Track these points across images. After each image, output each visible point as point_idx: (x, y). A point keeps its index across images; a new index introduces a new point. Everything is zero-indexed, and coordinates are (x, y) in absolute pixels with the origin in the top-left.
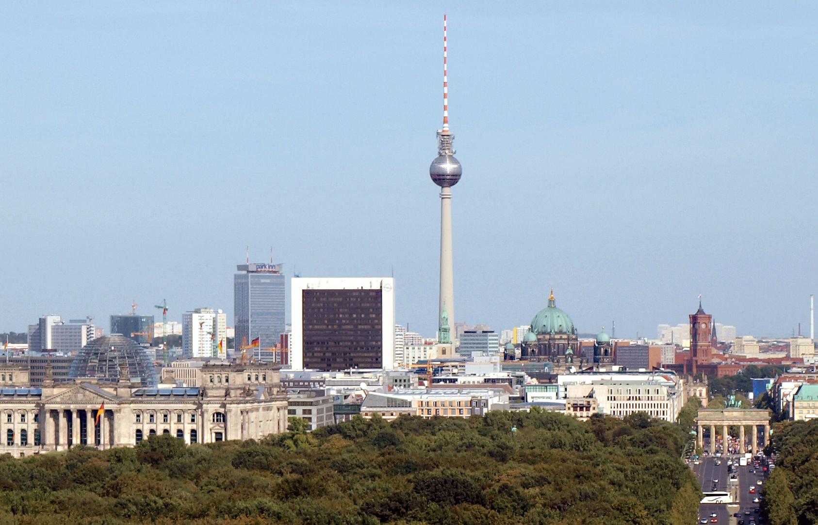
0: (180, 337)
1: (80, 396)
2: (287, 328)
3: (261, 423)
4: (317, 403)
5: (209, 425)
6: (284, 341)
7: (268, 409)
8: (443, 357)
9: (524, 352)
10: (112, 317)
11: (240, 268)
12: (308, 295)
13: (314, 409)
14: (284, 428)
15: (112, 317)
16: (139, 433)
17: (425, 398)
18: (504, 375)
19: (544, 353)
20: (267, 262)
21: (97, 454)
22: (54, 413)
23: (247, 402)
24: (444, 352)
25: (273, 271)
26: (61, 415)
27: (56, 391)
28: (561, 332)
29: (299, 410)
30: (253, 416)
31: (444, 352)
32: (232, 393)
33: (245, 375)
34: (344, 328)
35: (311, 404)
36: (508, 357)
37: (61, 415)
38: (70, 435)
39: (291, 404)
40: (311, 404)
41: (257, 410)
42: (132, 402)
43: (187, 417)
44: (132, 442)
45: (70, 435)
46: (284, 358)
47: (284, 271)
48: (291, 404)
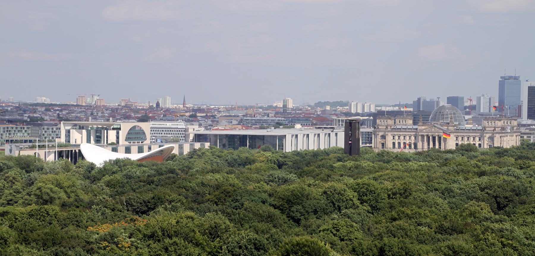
0: (475, 106)
1: (433, 130)
3: (510, 142)
5: (486, 142)
6: (520, 108)
7: (512, 136)
10: (449, 98)
11: (501, 77)
12: (530, 88)
13: (532, 137)
14: (519, 144)
15: (449, 98)
16: (457, 144)
20: (513, 75)
21: (440, 152)
22: (423, 136)
23: (502, 133)
25: (516, 78)
26: (425, 137)
27: (423, 127)
29: (525, 137)
30: (505, 139)
32: (497, 129)
33: (502, 122)
35: (531, 134)
37: (425, 137)
38: (429, 144)
40: (531, 134)
41: (507, 136)
43: (477, 139)
44: (454, 147)
45: (429, 144)
46: (520, 115)
47: (520, 79)
48: (522, 134)
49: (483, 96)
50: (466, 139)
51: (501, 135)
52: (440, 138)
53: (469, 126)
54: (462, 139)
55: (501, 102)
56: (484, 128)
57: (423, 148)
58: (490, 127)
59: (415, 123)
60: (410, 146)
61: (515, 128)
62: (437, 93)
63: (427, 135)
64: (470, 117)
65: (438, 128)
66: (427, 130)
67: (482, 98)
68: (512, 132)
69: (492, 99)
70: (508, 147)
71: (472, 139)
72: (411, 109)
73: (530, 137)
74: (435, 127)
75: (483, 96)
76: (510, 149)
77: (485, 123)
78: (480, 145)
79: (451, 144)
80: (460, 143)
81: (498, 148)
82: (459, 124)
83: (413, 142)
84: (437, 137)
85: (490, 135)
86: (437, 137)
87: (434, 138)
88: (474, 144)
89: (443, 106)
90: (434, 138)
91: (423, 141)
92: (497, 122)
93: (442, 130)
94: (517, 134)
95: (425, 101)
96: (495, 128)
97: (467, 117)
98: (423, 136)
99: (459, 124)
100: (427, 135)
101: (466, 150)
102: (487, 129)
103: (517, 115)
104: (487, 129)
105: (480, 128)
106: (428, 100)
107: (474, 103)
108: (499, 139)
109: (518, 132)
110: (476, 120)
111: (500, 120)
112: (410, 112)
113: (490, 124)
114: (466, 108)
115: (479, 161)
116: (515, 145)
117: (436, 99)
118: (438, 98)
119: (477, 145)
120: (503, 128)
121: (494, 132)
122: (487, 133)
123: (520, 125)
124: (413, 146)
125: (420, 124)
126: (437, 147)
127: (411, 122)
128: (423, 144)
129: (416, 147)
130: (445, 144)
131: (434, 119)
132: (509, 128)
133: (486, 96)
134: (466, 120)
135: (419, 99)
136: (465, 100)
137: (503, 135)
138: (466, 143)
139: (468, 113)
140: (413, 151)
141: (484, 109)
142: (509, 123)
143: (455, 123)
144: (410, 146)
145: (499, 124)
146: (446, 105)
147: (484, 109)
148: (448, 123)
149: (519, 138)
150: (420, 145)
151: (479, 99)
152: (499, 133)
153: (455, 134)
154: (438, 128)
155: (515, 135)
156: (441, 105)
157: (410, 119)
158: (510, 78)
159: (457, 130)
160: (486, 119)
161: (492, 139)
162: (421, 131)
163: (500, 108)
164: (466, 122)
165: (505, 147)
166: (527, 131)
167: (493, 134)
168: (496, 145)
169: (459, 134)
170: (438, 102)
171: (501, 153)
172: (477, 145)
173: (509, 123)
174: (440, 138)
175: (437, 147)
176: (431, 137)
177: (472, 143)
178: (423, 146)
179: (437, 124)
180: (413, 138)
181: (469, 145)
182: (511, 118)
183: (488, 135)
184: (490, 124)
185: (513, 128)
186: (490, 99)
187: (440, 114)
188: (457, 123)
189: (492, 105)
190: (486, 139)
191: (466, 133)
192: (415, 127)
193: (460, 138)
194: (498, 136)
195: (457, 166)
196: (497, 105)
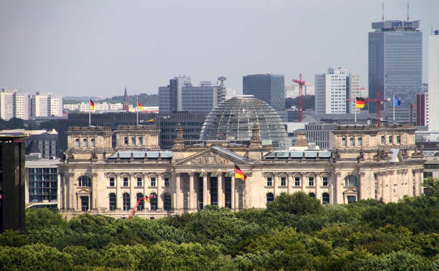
0: (313, 97)
1: (211, 160)
5: (341, 189)
7: (404, 172)
11: (375, 25)
14: (420, 191)
16: (270, 196)
20: (403, 19)
22: (185, 177)
23: (380, 165)
25: (410, 27)
27: (186, 155)
30: (387, 179)
32: (366, 156)
33: (379, 137)
38: (200, 198)
39: (426, 166)
41: (391, 173)
42: (264, 166)
43: (319, 181)
45: (200, 198)
47: (421, 28)
48: (426, 166)
49: (331, 72)
50: (291, 181)
51: (376, 170)
52: (227, 180)
53: (298, 150)
54: (283, 183)
55: (376, 87)
56: (336, 154)
57: (186, 208)
58: (350, 152)
59: (165, 144)
60: (154, 201)
61: (410, 153)
62: (219, 66)
63: (197, 175)
64: (301, 126)
65: (222, 155)
66: (196, 161)
67: (328, 78)
68: (404, 162)
69: (352, 80)
70: (395, 200)
71: (305, 181)
72: (155, 109)
74: (215, 152)
75: (331, 72)
76: (400, 206)
77: (338, 141)
78: (326, 196)
79: (256, 195)
80: (278, 192)
81: (371, 202)
82: (276, 145)
83: (160, 192)
84: (220, 179)
85: (351, 170)
86: (220, 179)
87: (213, 182)
88: (312, 195)
89: (234, 100)
90: (213, 182)
91: (185, 189)
92: (366, 137)
93: (232, 159)
94: (414, 167)
95: (188, 87)
97: (293, 127)
98: (185, 177)
99: (276, 145)
101: (290, 209)
102: (343, 156)
103: (415, 119)
104: (343, 156)
105: (325, 153)
106: (196, 84)
107: (310, 90)
108: (373, 181)
109: (418, 163)
110: (313, 134)
111: (373, 134)
112: (152, 115)
113: (349, 142)
114: (289, 102)
115: (325, 237)
116: (411, 195)
117: (214, 82)
118: (222, 79)
119: (319, 197)
120: (381, 154)
121: (359, 164)
122: (342, 166)
124: (161, 203)
125: (178, 146)
127: (152, 141)
128: (186, 196)
129: (168, 206)
130: (241, 196)
131: (212, 132)
132: (396, 152)
133: (337, 72)
134: (291, 135)
135: (174, 83)
136: (288, 83)
137: (382, 170)
138: (292, 191)
139: (295, 117)
140: (161, 215)
141: (333, 105)
142: (395, 140)
144: (154, 201)
145: (372, 142)
146: (241, 96)
147: (333, 105)
148: (248, 143)
149: (420, 177)
150: (178, 200)
151: (321, 81)
153: (265, 170)
154: (222, 155)
155: (410, 169)
156: (228, 97)
157: (153, 134)
158: (396, 25)
159: (271, 161)
160: (339, 131)
161: (354, 180)
163: (374, 101)
164: (290, 139)
165: (387, 201)
170: (221, 91)
171: (380, 215)
172: (319, 197)
173: (395, 140)
174: (227, 180)
175: (221, 203)
176: (205, 179)
178: (186, 202)
179: (220, 145)
180: (161, 182)
181: (300, 196)
182: (400, 129)
183: (344, 172)
184: (349, 142)
185: (404, 151)
186: (348, 79)
187: (226, 119)
189: (353, 96)
190: (341, 180)
191: (292, 166)
192: (166, 154)
193: (278, 181)
194: (369, 173)
195: (271, 251)
196: (365, 94)
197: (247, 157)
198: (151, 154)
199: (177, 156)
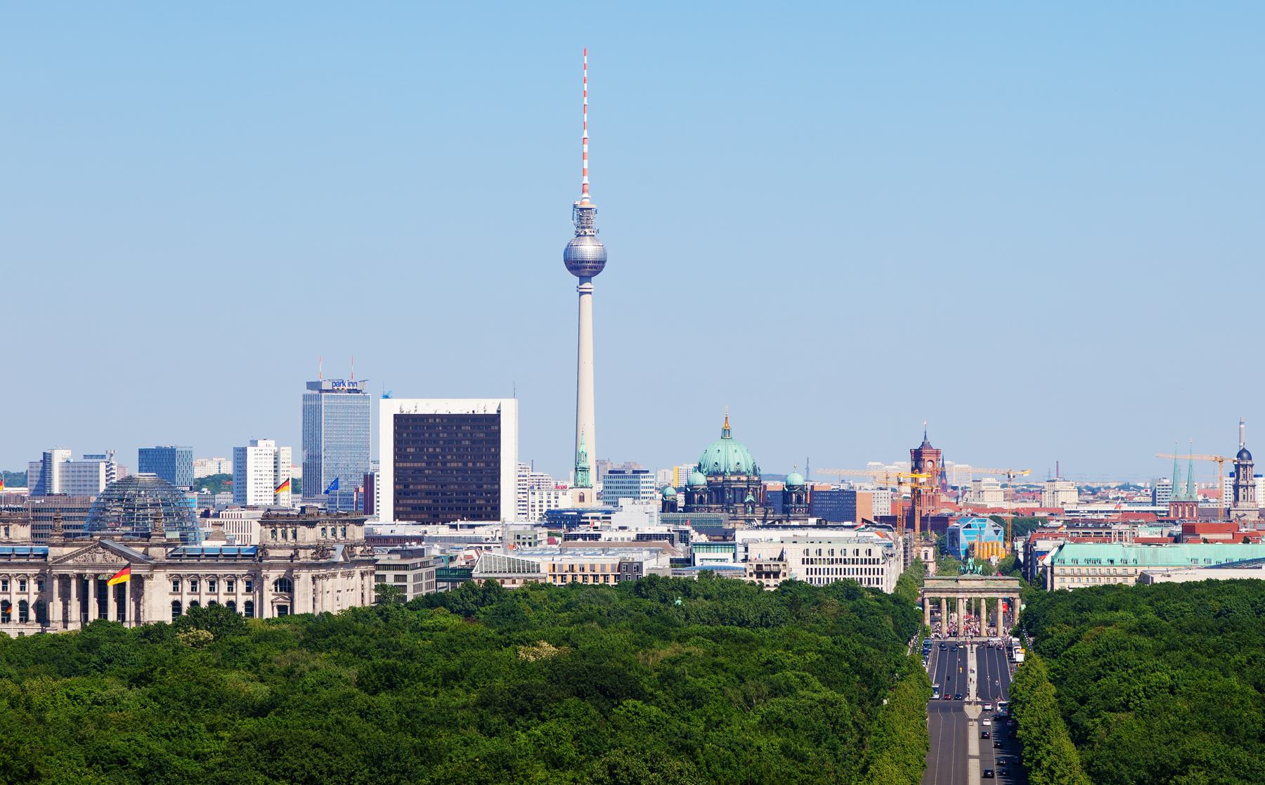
2: (372, 466)
4: (414, 567)
5: (269, 596)
6: (369, 481)
7: (350, 575)
8: (580, 506)
9: (689, 498)
10: (141, 452)
14: (370, 599)
16: (177, 606)
17: (557, 560)
18: (663, 529)
19: (718, 499)
22: (65, 580)
23: (320, 566)
24: (582, 499)
26: (74, 582)
27: (67, 551)
28: (738, 473)
30: (328, 584)
31: (582, 499)
32: (302, 553)
33: (318, 528)
34: (450, 465)
35: (406, 567)
36: (669, 506)
37: (74, 582)
38: (84, 609)
39: (379, 567)
40: (406, 567)
41: (334, 575)
43: (241, 586)
45: (84, 609)
46: (368, 505)
47: (366, 388)
48: (379, 567)
51: (315, 572)
58: (280, 548)
61: (358, 550)
63: (80, 577)
66: (80, 559)
71: (223, 586)
73: (404, 578)
74: (105, 547)
78: (249, 605)
79: (157, 604)
83: (32, 600)
85: (281, 573)
91: (65, 597)
92: (302, 530)
94: (363, 568)
96: (296, 548)
98: (65, 580)
99: (184, 539)
100: (80, 577)
102: (272, 553)
104: (272, 553)
108: (311, 587)
116: (358, 605)
119: (241, 608)
120: (321, 550)
121: (293, 564)
122: (271, 566)
123: (374, 540)
126: (112, 615)
127: (22, 533)
128: (65, 605)
129: (43, 618)
130: (138, 605)
132: (340, 548)
137: (322, 571)
140: (32, 629)
143: (170, 535)
145: (309, 535)
146: (136, 474)
149: (370, 581)
152: (308, 566)
153: (169, 571)
154: (114, 551)
155: (357, 571)
159: (175, 560)
161: (286, 585)
162: (60, 561)
166: (396, 560)
167: (291, 571)
168: (299, 610)
169: (182, 572)
171: (321, 631)
172: (241, 608)
175: (112, 615)
176: (91, 583)
177: (223, 600)
179: (111, 537)
180: (33, 587)
183: (273, 575)
185: (350, 547)
188: (176, 535)
190: (268, 585)
191: (206, 566)
193: (187, 586)
196: (298, 473)
197: (146, 553)
198: (20, 550)
199: (54, 552)
